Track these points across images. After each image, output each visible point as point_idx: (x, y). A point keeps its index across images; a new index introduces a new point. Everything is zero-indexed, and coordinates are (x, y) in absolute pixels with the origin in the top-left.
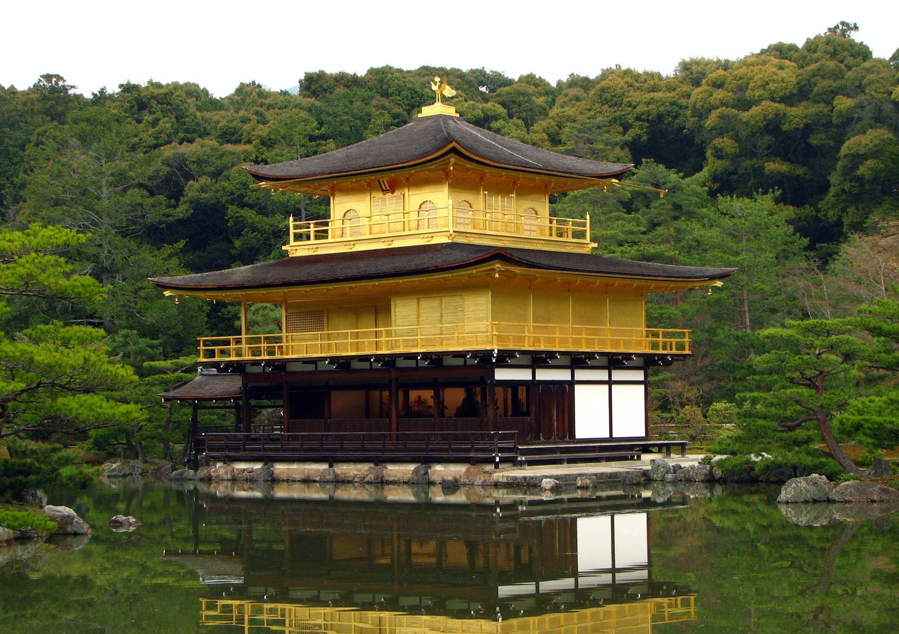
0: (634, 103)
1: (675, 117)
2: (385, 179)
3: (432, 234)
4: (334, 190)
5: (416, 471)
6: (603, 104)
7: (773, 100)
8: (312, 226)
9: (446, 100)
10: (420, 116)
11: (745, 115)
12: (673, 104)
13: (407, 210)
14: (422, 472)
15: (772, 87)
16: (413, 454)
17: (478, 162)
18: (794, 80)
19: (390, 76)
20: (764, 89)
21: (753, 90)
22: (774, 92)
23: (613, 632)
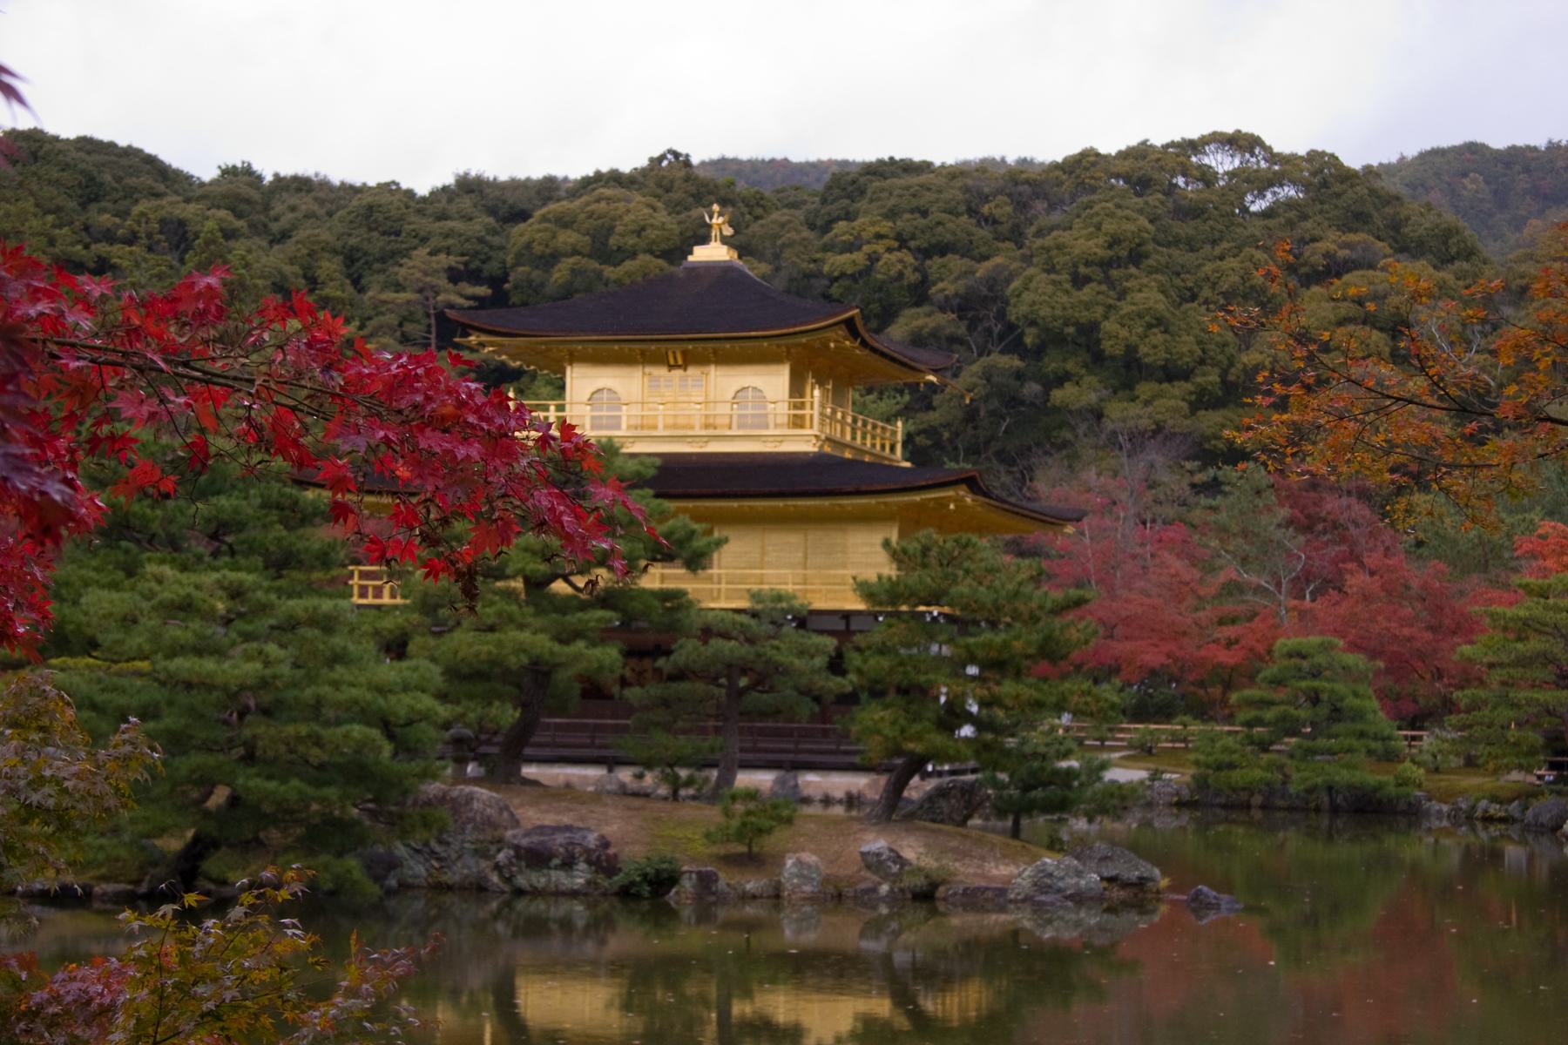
0: (422, 233)
1: (484, 262)
2: (678, 348)
3: (781, 438)
4: (574, 358)
5: (779, 782)
6: (371, 230)
7: (651, 252)
8: (552, 408)
9: (725, 240)
10: (690, 258)
11: (609, 272)
12: (481, 240)
13: (711, 398)
14: (792, 783)
15: (652, 234)
16: (771, 757)
17: (864, 344)
18: (676, 229)
19: (47, 147)
20: (639, 236)
21: (622, 235)
22: (654, 242)
23: (828, 1016)
